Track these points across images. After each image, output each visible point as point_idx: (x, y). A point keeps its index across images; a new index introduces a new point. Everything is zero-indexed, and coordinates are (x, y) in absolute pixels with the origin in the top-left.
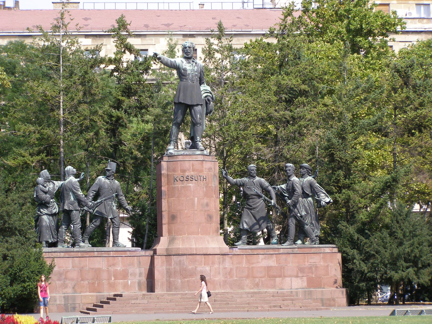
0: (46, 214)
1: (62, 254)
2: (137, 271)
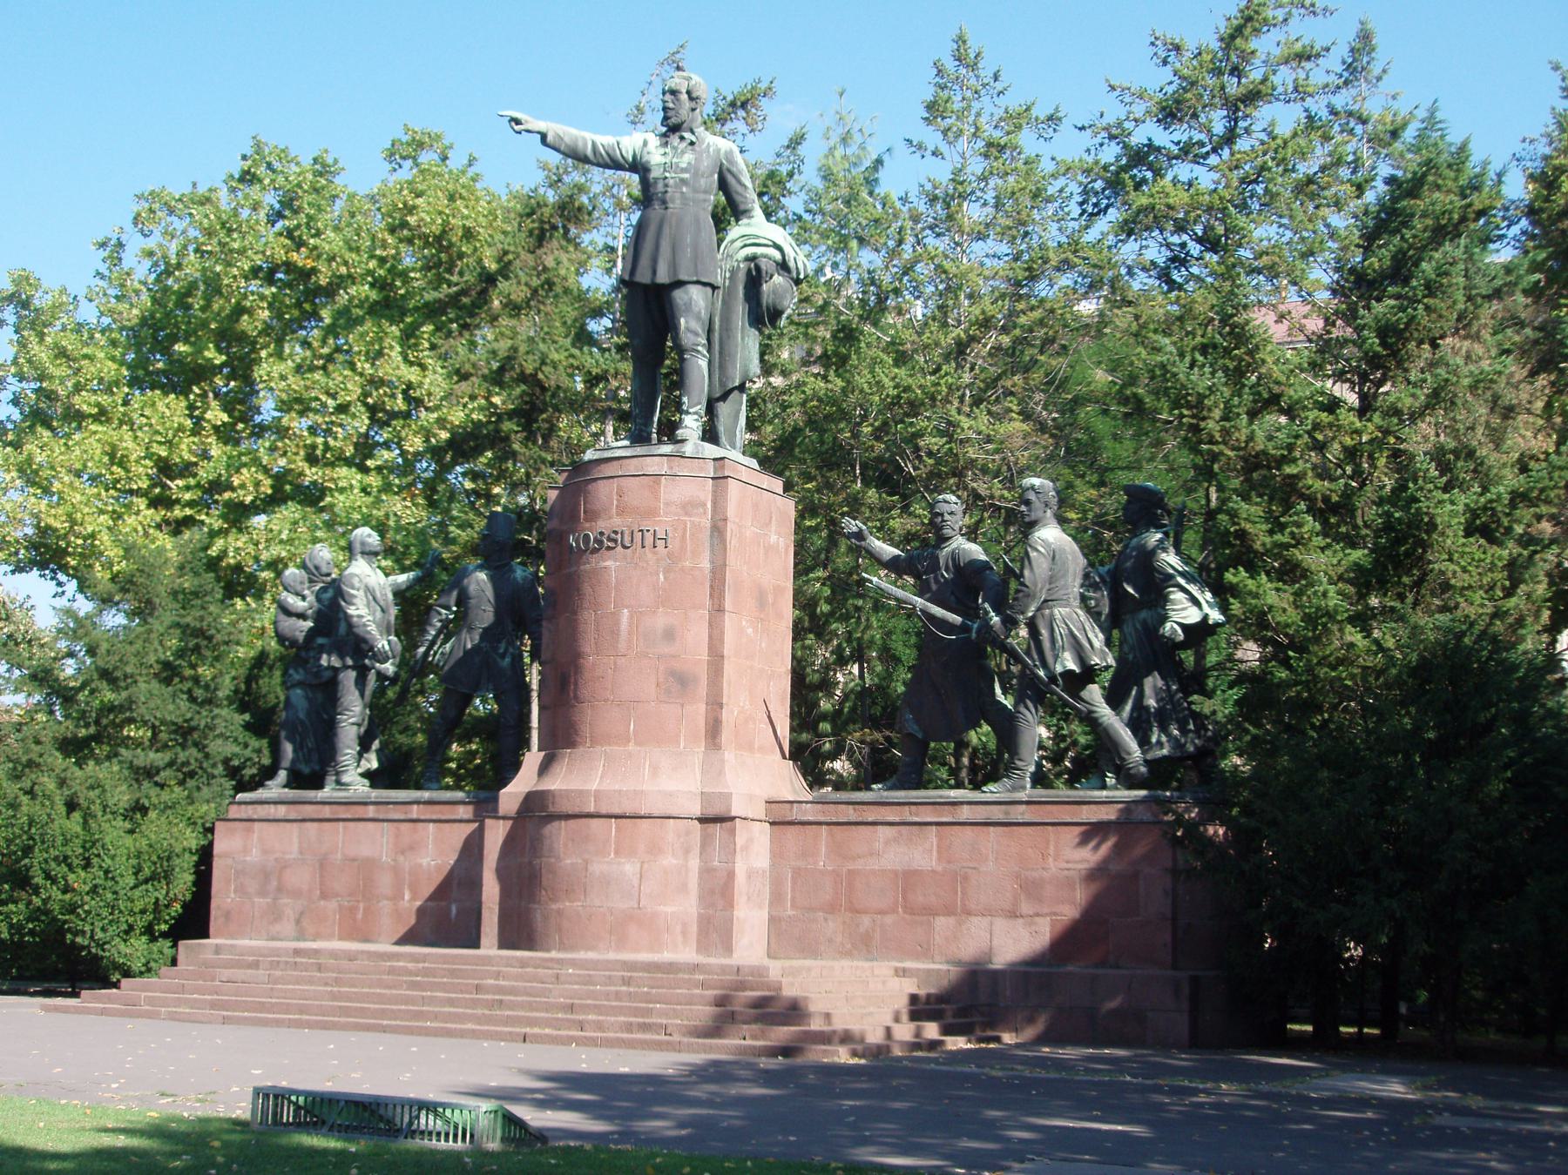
1: (281, 811)
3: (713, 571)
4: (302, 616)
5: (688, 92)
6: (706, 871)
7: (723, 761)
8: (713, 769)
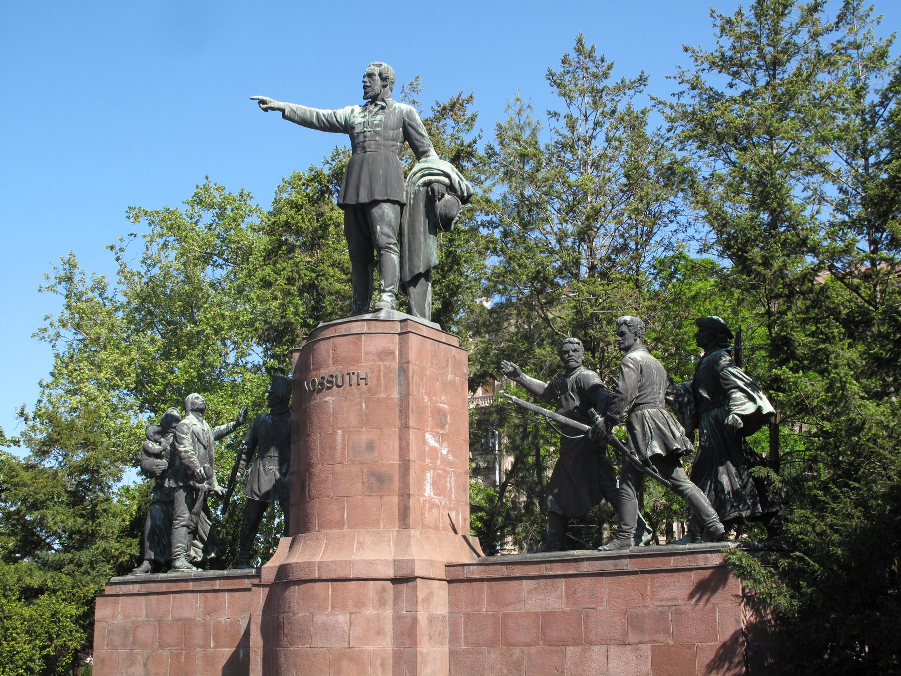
1: (136, 588)
3: (401, 400)
4: (158, 456)
5: (380, 75)
6: (397, 618)
7: (409, 536)
8: (403, 544)
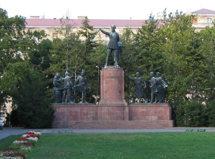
0: (58, 90)
1: (63, 106)
2: (92, 112)
